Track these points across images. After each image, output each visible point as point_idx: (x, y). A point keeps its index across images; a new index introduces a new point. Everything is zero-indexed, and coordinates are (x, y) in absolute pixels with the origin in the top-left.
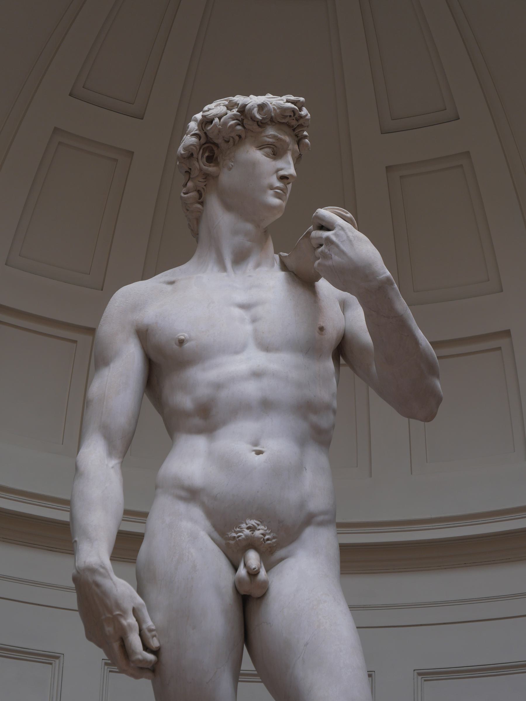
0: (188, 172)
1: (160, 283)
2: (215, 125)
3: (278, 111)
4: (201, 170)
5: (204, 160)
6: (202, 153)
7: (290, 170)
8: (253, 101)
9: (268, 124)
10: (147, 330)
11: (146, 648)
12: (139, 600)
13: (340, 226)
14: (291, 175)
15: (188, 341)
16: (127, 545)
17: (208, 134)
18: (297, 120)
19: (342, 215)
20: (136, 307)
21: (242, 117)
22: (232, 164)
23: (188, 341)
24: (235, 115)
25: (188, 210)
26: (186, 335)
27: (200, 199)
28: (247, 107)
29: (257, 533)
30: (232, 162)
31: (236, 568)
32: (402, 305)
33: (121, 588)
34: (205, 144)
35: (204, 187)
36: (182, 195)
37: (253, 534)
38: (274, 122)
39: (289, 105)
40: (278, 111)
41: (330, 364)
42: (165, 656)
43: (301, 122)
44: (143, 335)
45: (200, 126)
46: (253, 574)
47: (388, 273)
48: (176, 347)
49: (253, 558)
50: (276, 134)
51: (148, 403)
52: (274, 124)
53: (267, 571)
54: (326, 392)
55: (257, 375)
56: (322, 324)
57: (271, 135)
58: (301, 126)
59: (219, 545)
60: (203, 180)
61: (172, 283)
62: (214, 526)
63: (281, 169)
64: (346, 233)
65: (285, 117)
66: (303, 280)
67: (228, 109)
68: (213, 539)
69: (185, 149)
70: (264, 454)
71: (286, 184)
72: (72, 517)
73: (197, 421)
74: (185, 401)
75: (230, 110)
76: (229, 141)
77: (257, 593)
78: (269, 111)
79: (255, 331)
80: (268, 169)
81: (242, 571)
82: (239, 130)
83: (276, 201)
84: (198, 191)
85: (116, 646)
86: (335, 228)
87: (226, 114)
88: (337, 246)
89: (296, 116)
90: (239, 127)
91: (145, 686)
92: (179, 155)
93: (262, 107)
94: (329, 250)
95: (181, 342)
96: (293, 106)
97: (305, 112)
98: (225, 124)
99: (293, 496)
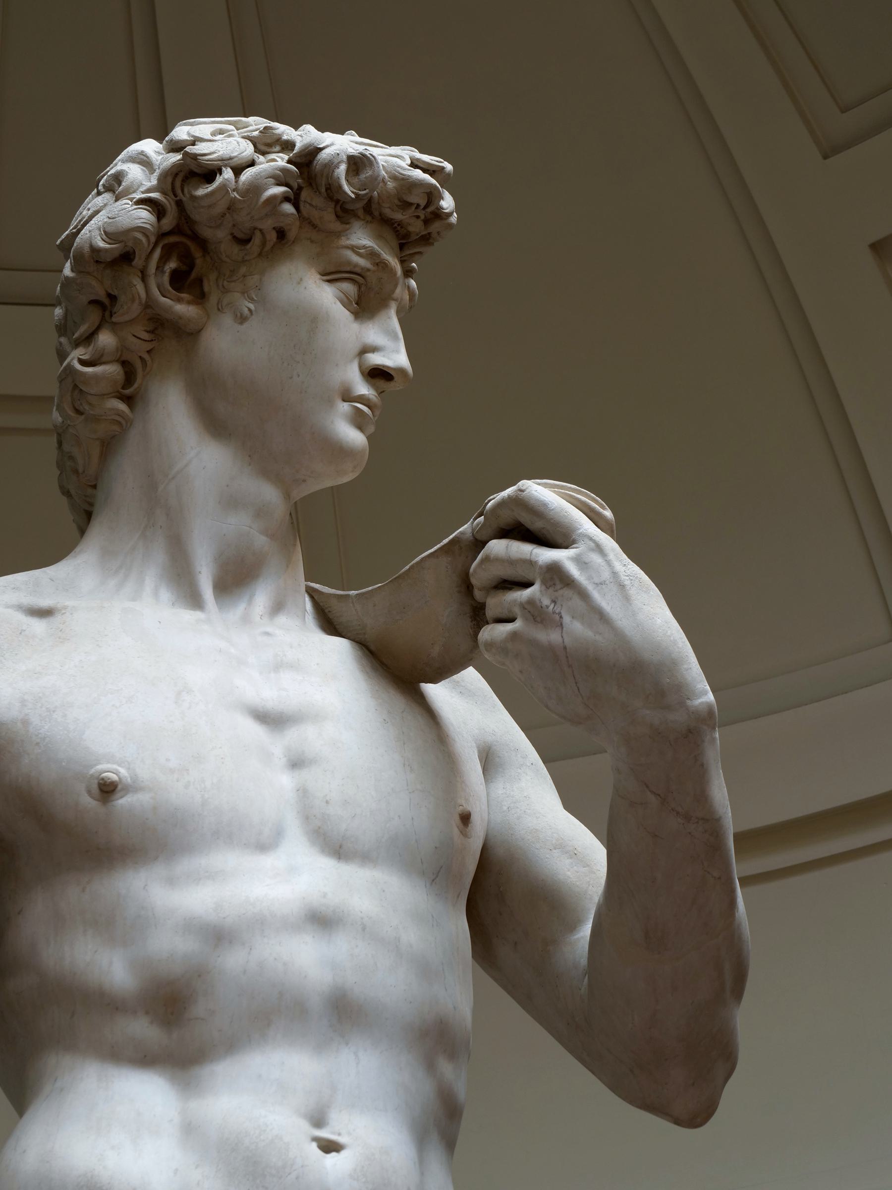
1: (8, 606)
2: (224, 187)
3: (391, 185)
5: (166, 278)
6: (161, 259)
7: (396, 357)
9: (357, 217)
13: (591, 539)
14: (401, 371)
18: (427, 222)
19: (592, 510)
24: (284, 170)
26: (123, 771)
27: (123, 388)
28: (323, 155)
30: (252, 300)
35: (146, 356)
36: (78, 366)
39: (418, 174)
40: (391, 185)
43: (435, 227)
45: (170, 179)
47: (710, 697)
48: (88, 802)
50: (376, 247)
52: (369, 218)
55: (321, 920)
57: (364, 247)
58: (426, 239)
60: (145, 336)
61: (44, 613)
63: (374, 349)
64: (609, 563)
65: (405, 205)
66: (401, 669)
67: (257, 150)
69: (109, 236)
70: (344, 1154)
71: (381, 393)
73: (141, 1029)
74: (112, 967)
75: (264, 154)
79: (303, 793)
82: (288, 215)
83: (354, 437)
84: (125, 364)
86: (574, 542)
87: (252, 164)
88: (583, 594)
89: (431, 209)
90: (288, 208)
92: (87, 249)
93: (358, 163)
94: (554, 602)
95: (107, 790)
96: (427, 177)
97: (447, 202)
98: (255, 189)
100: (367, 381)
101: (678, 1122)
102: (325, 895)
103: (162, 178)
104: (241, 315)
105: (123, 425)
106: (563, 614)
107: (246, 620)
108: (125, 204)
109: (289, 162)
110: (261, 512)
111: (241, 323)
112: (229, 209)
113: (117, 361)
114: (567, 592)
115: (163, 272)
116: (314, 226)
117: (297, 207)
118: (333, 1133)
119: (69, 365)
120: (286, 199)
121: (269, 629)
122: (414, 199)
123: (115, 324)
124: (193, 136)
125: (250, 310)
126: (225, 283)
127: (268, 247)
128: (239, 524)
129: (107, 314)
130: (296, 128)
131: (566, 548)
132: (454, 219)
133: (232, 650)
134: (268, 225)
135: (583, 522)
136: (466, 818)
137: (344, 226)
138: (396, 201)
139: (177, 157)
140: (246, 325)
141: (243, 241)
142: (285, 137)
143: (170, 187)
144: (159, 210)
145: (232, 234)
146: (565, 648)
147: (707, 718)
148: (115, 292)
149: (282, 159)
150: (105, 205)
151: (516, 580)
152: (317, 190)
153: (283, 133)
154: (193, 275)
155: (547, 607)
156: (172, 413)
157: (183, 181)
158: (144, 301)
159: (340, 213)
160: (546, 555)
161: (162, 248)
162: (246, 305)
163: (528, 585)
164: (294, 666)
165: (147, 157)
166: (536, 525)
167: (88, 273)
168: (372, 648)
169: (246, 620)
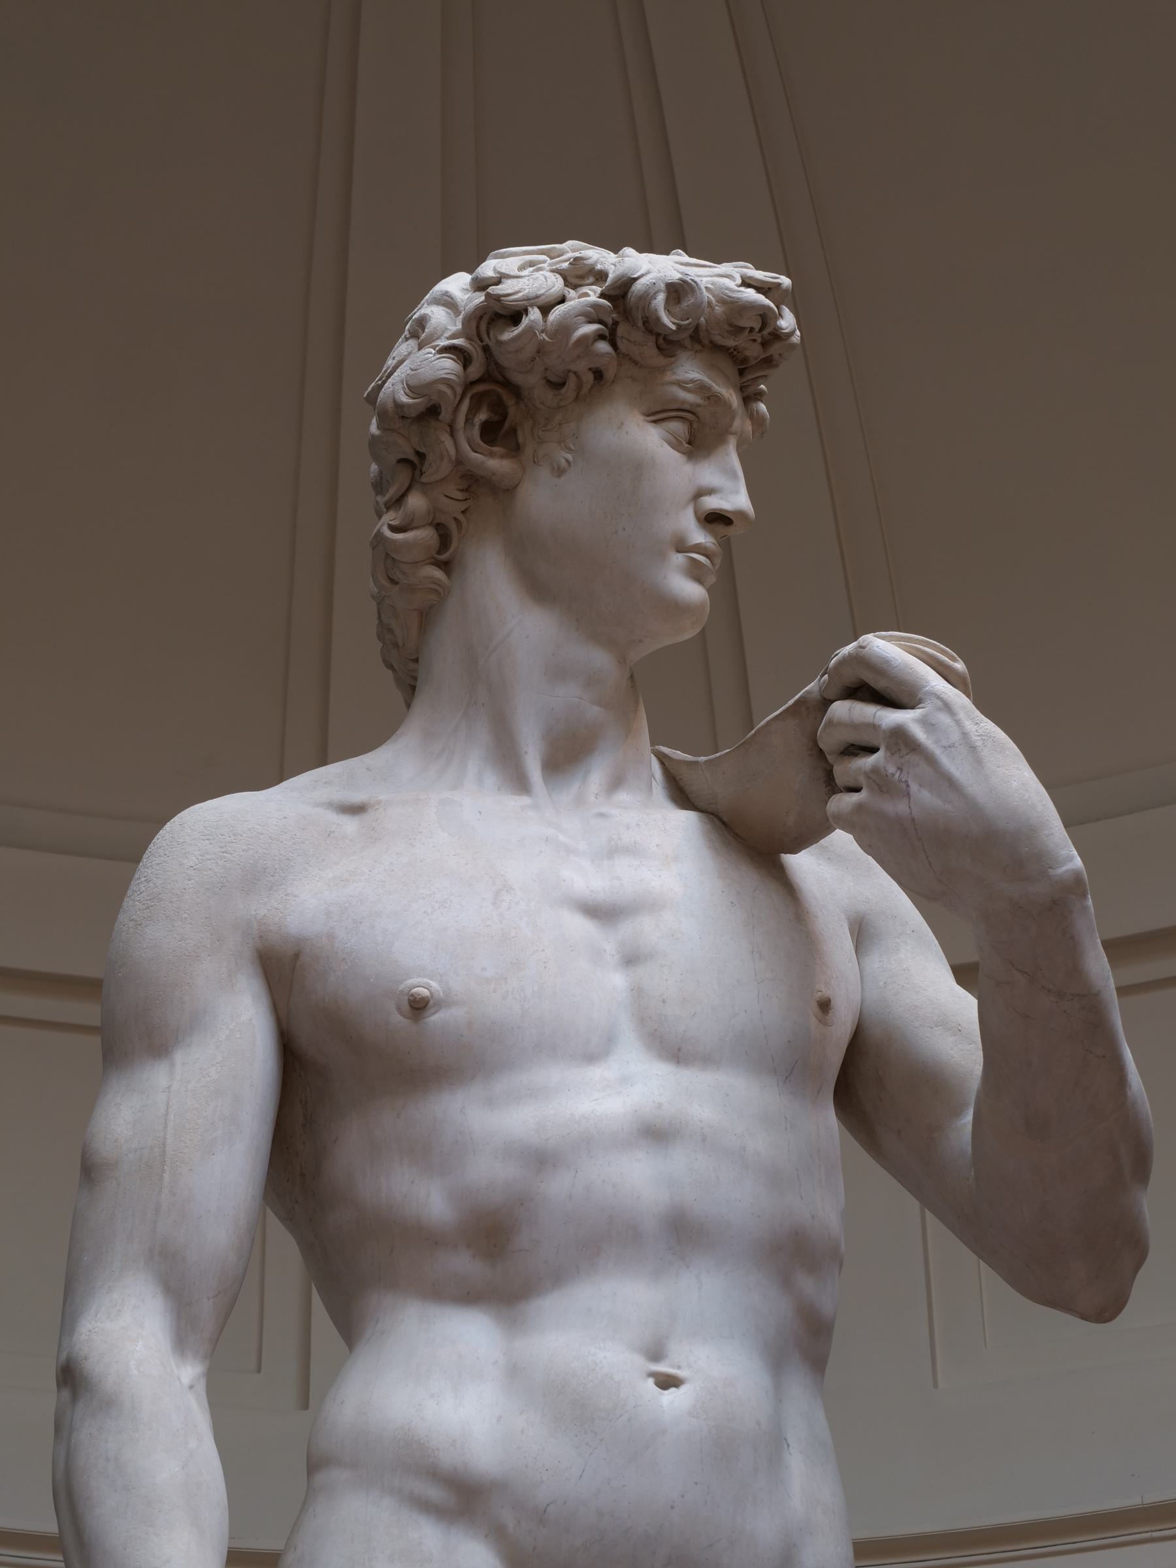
1: (318, 805)
2: (530, 329)
3: (719, 309)
4: (459, 462)
5: (476, 432)
8: (655, 268)
9: (684, 348)
10: (297, 956)
13: (938, 697)
14: (741, 514)
15: (440, 1004)
17: (496, 351)
18: (765, 344)
19: (941, 663)
20: (256, 877)
21: (614, 315)
22: (569, 457)
23: (440, 1004)
24: (595, 306)
25: (393, 582)
26: (434, 984)
27: (439, 553)
28: (638, 286)
30: (569, 450)
34: (479, 381)
35: (461, 517)
38: (699, 342)
39: (751, 294)
40: (719, 309)
43: (775, 349)
44: (283, 970)
45: (474, 324)
47: (1078, 862)
48: (398, 1020)
50: (706, 379)
52: (698, 347)
54: (823, 1208)
55: (655, 1133)
56: (827, 992)
57: (692, 381)
58: (768, 362)
60: (459, 495)
61: (355, 809)
63: (710, 491)
64: (958, 723)
65: (737, 330)
66: (755, 843)
67: (567, 283)
69: (413, 389)
70: (684, 1389)
73: (463, 1264)
74: (430, 1199)
75: (575, 287)
76: (562, 384)
79: (638, 992)
80: (672, 485)
82: (603, 355)
83: (691, 591)
84: (439, 526)
86: (920, 701)
87: (562, 300)
88: (930, 760)
89: (765, 332)
90: (603, 347)
92: (390, 405)
93: (678, 291)
94: (900, 769)
95: (418, 1007)
96: (761, 298)
97: (787, 321)
98: (564, 329)
100: (704, 527)
101: (1084, 1317)
102: (660, 1106)
103: (467, 321)
104: (559, 468)
105: (440, 594)
106: (910, 782)
107: (580, 801)
108: (429, 352)
109: (602, 296)
111: (559, 476)
112: (538, 352)
113: (430, 524)
114: (913, 758)
115: (473, 425)
116: (636, 363)
117: (614, 345)
118: (672, 1366)
119: (379, 531)
120: (600, 337)
121: (604, 810)
122: (746, 323)
123: (425, 484)
124: (499, 273)
125: (567, 461)
126: (540, 433)
127: (585, 390)
128: (569, 695)
129: (417, 472)
130: (616, 252)
131: (913, 708)
132: (796, 338)
133: (561, 838)
134: (582, 366)
135: (929, 678)
136: (825, 1006)
137: (668, 360)
138: (726, 327)
139: (480, 298)
140: (563, 478)
141: (557, 385)
142: (599, 267)
143: (474, 332)
144: (465, 358)
145: (545, 378)
146: (913, 820)
147: (1076, 886)
148: (423, 450)
149: (595, 292)
150: (410, 353)
151: (863, 744)
152: (634, 324)
153: (596, 262)
154: (507, 425)
155: (893, 775)
156: (490, 577)
157: (489, 324)
158: (454, 458)
159: (664, 346)
160: (891, 717)
161: (471, 398)
162: (563, 456)
163: (873, 750)
164: (632, 850)
165: (450, 296)
166: (879, 684)
167: (394, 430)
168: (725, 819)
169: (580, 801)
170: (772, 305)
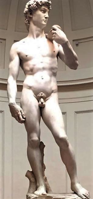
0: (26, 17)
4: (29, 16)
11: (23, 118)
12: (21, 109)
16: (19, 99)
20: (17, 48)
28: (38, 2)
29: (43, 95)
31: (39, 102)
32: (70, 46)
33: (18, 107)
37: (42, 95)
41: (56, 59)
42: (27, 119)
44: (19, 54)
46: (42, 103)
48: (25, 57)
49: (42, 100)
51: (21, 68)
53: (45, 102)
54: (55, 65)
56: (54, 50)
58: (49, 5)
59: (35, 97)
62: (35, 94)
66: (50, 40)
68: (34, 96)
71: (46, 19)
72: (8, 83)
73: (30, 72)
74: (28, 68)
77: (43, 107)
78: (43, 3)
80: (43, 16)
81: (40, 103)
85: (17, 118)
90: (36, 7)
91: (23, 124)
95: (27, 56)
98: (34, 6)
99: (49, 87)
110: (39, 31)
128: (37, 32)
147: (67, 42)
162: (35, 15)
170: (48, 1)
